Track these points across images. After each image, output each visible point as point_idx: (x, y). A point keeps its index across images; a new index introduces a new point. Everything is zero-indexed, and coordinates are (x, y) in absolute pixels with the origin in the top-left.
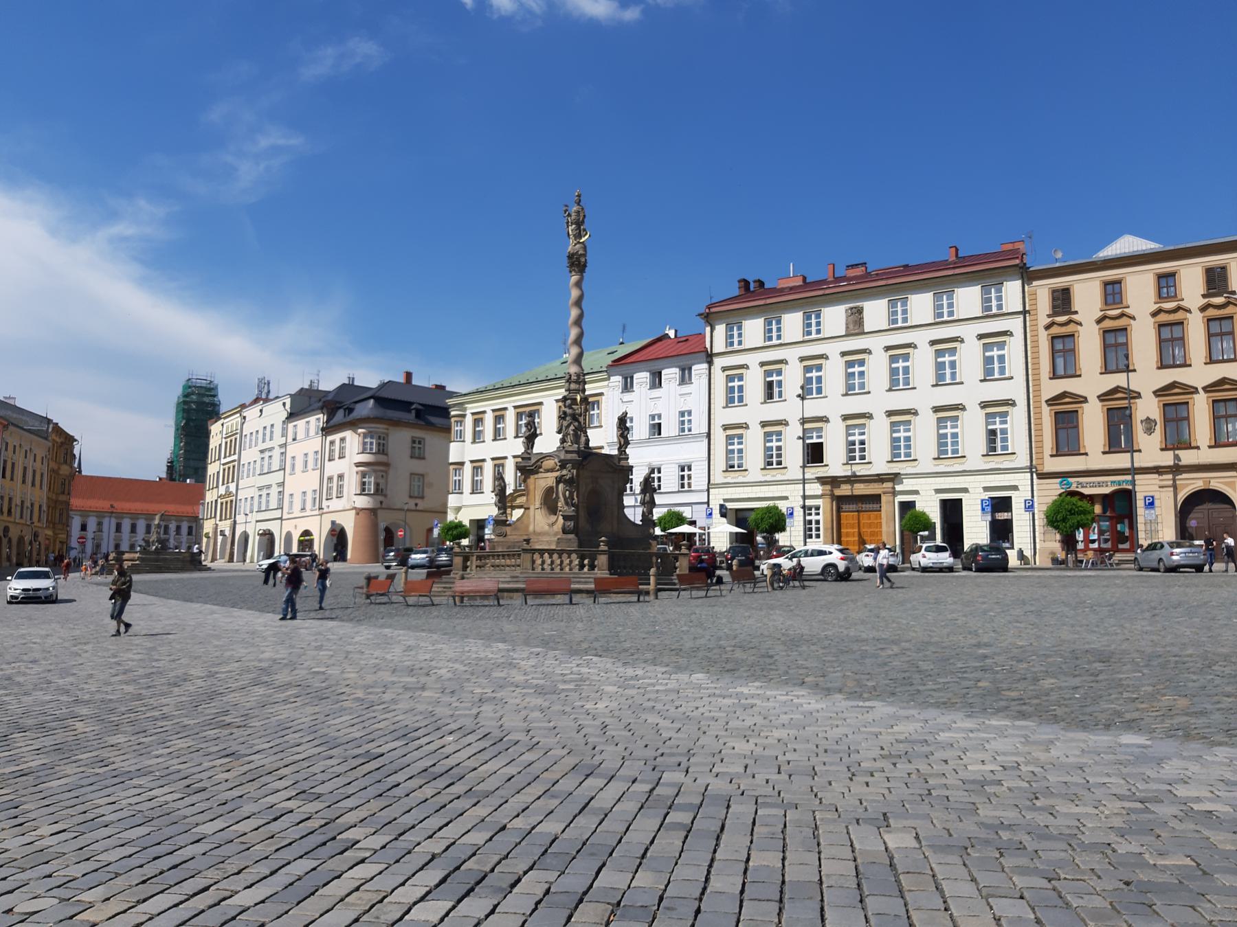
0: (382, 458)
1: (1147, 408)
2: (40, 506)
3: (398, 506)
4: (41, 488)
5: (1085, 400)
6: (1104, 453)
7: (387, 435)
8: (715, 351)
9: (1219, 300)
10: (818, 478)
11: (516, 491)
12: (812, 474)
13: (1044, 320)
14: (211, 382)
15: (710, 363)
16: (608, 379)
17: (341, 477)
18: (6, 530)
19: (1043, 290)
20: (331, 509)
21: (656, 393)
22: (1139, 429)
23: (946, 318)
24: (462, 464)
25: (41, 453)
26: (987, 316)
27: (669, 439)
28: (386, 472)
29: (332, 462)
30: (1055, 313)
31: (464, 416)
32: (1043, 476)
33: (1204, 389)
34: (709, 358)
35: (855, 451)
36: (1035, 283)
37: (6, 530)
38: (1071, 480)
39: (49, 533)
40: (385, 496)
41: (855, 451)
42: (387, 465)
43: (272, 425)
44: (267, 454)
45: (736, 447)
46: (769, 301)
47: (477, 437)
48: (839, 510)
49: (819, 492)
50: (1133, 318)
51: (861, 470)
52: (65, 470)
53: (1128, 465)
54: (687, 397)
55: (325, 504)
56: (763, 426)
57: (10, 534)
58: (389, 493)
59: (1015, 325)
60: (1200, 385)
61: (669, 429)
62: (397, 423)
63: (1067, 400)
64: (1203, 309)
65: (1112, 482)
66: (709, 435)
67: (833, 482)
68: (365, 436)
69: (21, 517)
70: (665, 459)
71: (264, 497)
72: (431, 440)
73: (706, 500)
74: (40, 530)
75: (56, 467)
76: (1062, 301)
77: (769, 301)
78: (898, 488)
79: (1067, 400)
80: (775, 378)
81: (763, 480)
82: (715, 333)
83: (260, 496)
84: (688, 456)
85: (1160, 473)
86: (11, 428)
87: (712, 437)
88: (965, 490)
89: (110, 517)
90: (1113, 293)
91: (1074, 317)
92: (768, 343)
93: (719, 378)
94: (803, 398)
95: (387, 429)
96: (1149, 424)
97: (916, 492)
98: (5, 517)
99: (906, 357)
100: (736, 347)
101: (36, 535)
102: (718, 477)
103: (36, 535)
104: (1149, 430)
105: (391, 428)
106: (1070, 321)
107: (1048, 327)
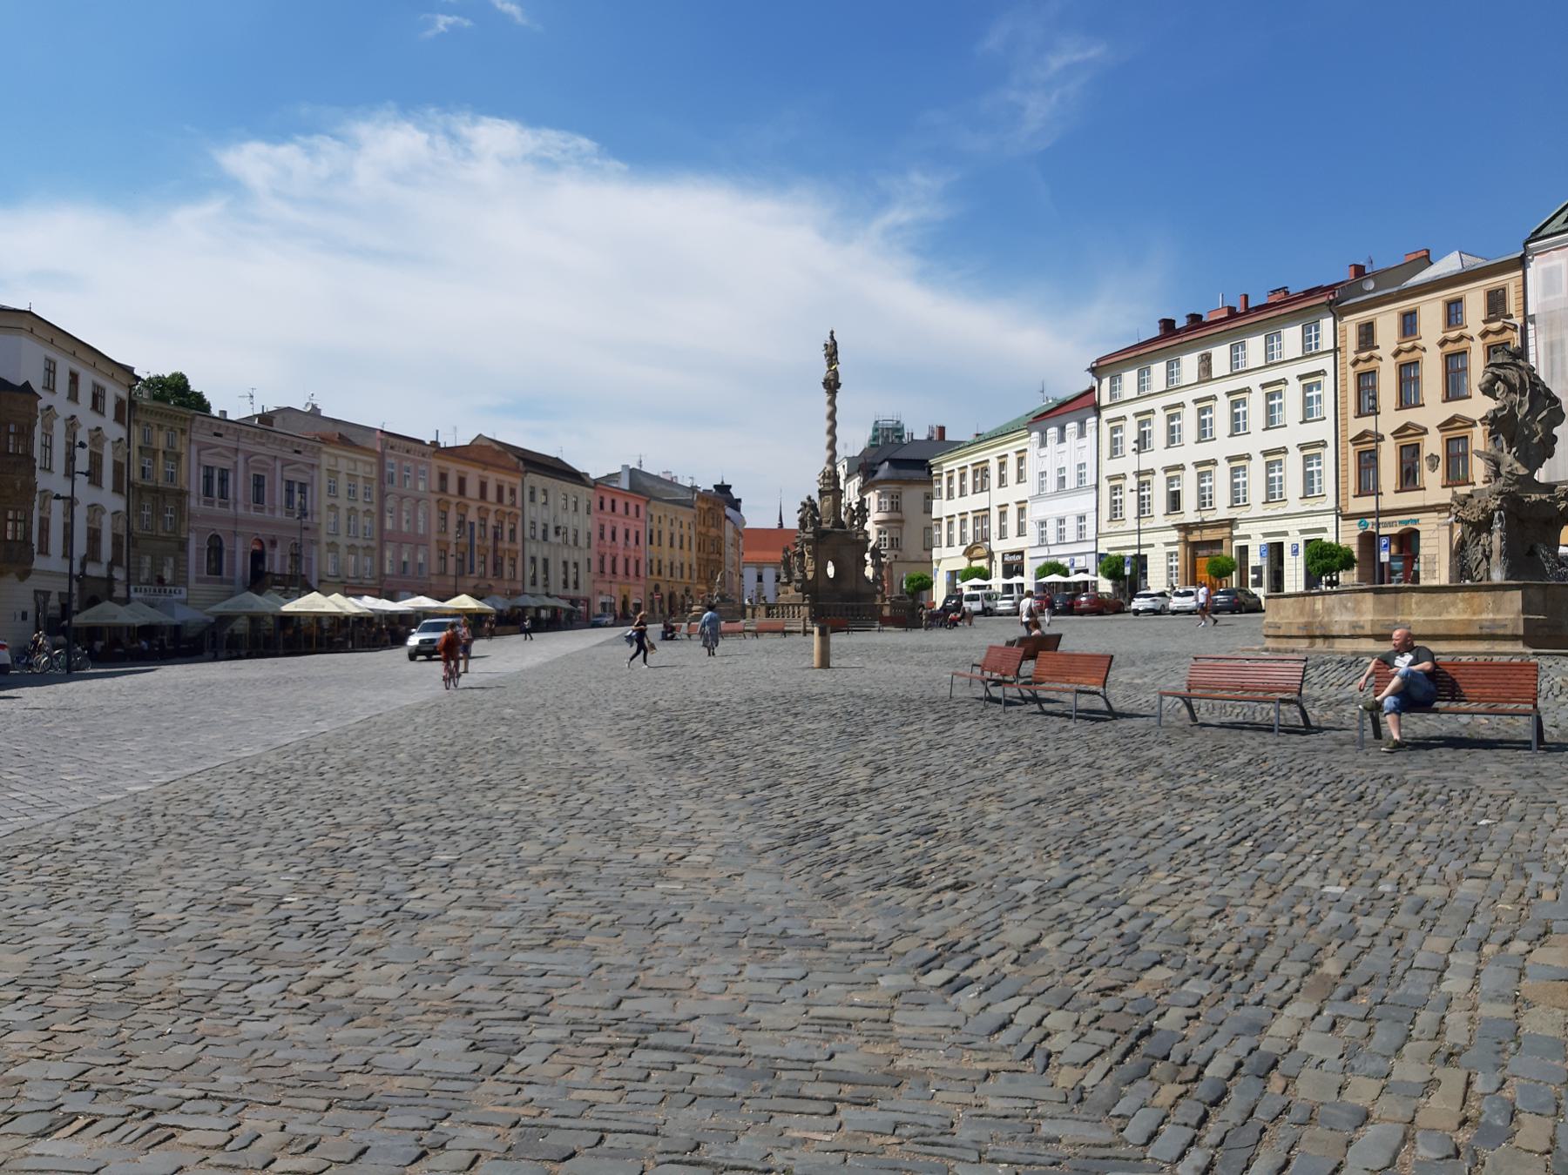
0: (896, 515)
1: (1433, 444)
2: (690, 566)
3: (913, 558)
4: (690, 549)
5: (1425, 431)
6: (1396, 492)
9: (1496, 326)
11: (974, 543)
13: (1351, 357)
14: (898, 422)
15: (1098, 415)
16: (1030, 435)
18: (657, 587)
19: (1351, 323)
22: (1424, 465)
23: (1275, 360)
24: (941, 519)
25: (686, 520)
26: (1307, 355)
27: (1071, 491)
28: (901, 529)
30: (1361, 350)
31: (941, 475)
32: (1348, 517)
33: (1481, 420)
34: (1097, 410)
35: (1204, 501)
36: (1346, 319)
37: (657, 587)
38: (1369, 520)
39: (703, 587)
40: (901, 550)
41: (1204, 501)
42: (901, 521)
45: (1277, 474)
46: (1232, 326)
47: (950, 495)
48: (1194, 556)
49: (1176, 539)
50: (1424, 350)
51: (1209, 516)
52: (713, 532)
53: (1373, 508)
56: (1302, 449)
57: (661, 591)
58: (904, 547)
59: (1326, 363)
60: (1477, 415)
61: (1071, 483)
62: (910, 482)
63: (1458, 424)
64: (1484, 335)
65: (1400, 522)
66: (1097, 487)
67: (1185, 528)
68: (880, 496)
69: (672, 575)
72: (912, 496)
74: (691, 587)
75: (703, 530)
76: (1367, 335)
77: (1232, 326)
78: (1236, 533)
79: (1458, 424)
80: (1147, 428)
82: (1102, 386)
85: (1439, 512)
86: (653, 502)
88: (1285, 534)
90: (1409, 323)
91: (1465, 331)
92: (1142, 394)
93: (1105, 429)
94: (1139, 452)
96: (1433, 459)
97: (1248, 537)
98: (655, 576)
99: (1244, 401)
101: (687, 590)
102: (1104, 528)
103: (687, 590)
104: (1433, 468)
106: (1371, 358)
107: (1355, 363)
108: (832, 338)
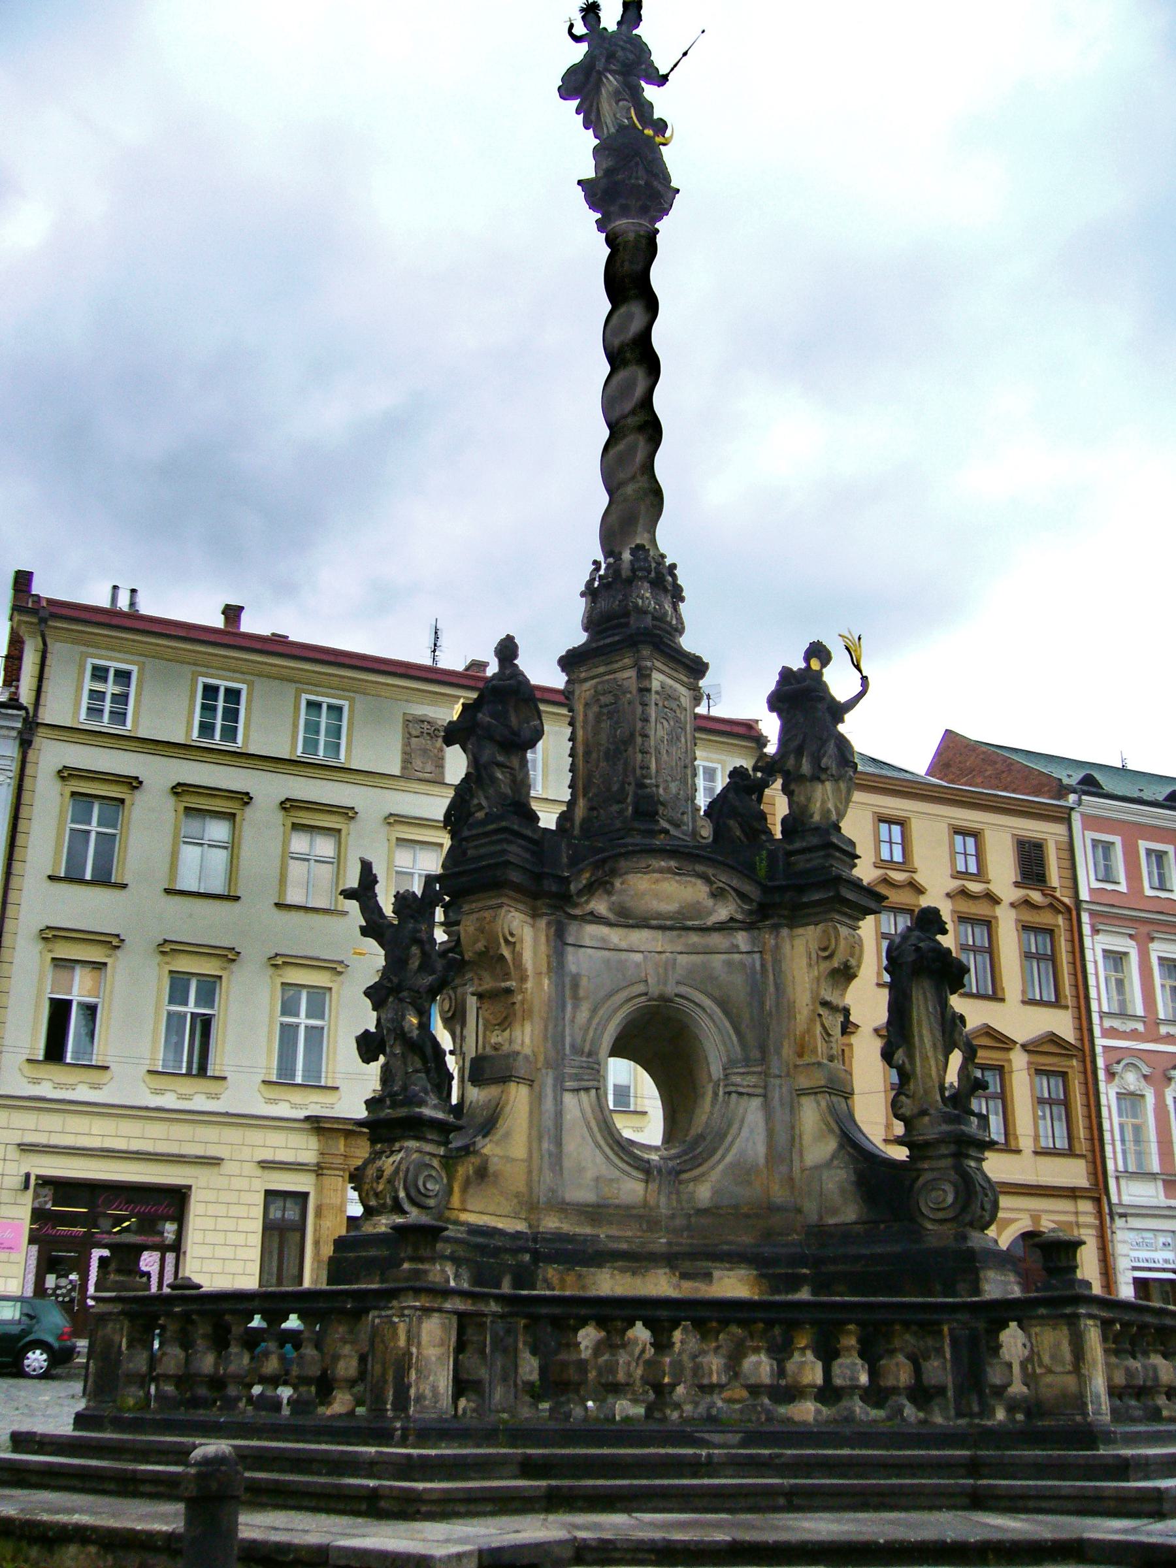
8: (48, 715)
10: (308, 1119)
12: (294, 1106)
15: (25, 745)
33: (1023, 1046)
81: (152, 1105)
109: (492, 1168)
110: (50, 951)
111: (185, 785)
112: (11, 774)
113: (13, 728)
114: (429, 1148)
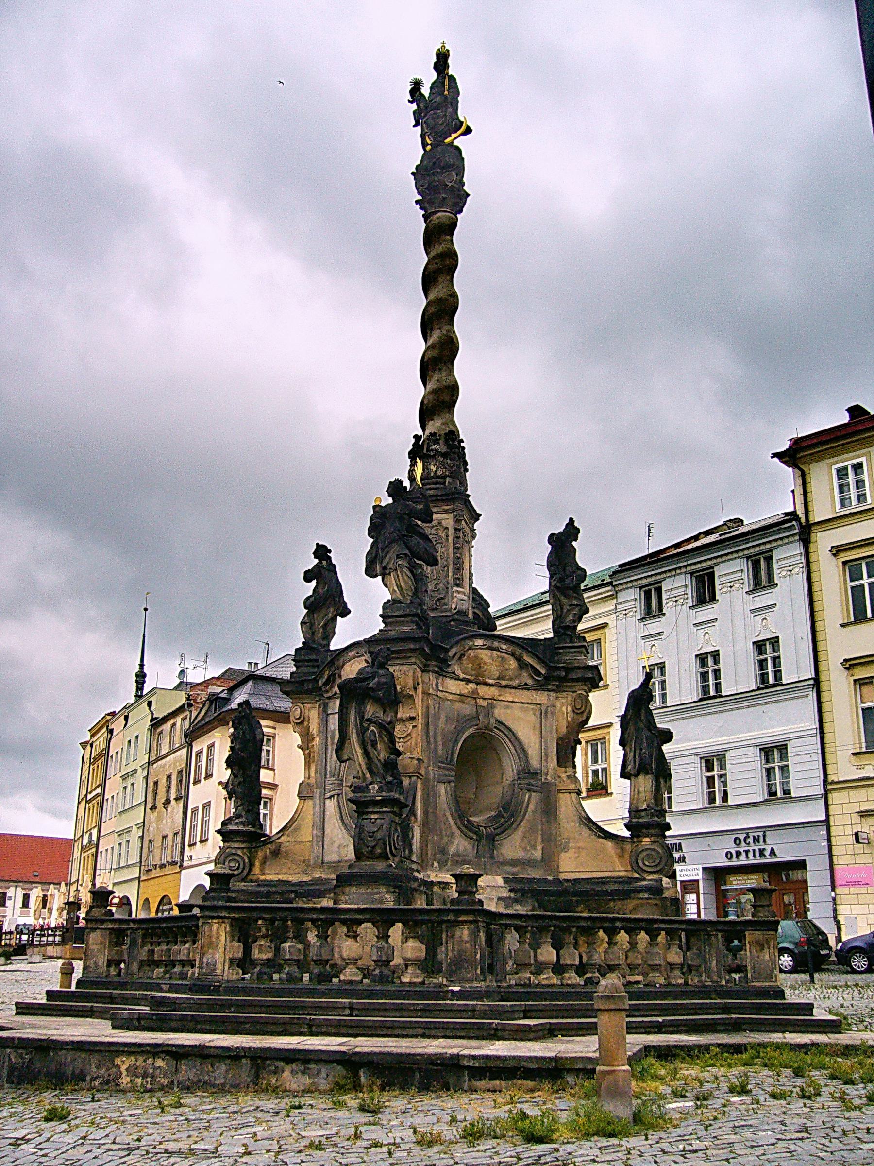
7: (274, 737)
15: (806, 542)
17: (206, 806)
20: (193, 863)
21: (706, 613)
27: (739, 698)
29: (198, 786)
43: (137, 737)
44: (130, 781)
54: (769, 616)
55: (187, 851)
66: (817, 683)
70: (732, 738)
71: (124, 845)
73: (823, 818)
83: (120, 844)
84: (778, 730)
87: (824, 687)
89: (16, 887)
95: (274, 728)
100: (854, 506)
105: (278, 725)
108: (442, 61)
109: (283, 850)
110: (852, 675)
111: (837, 547)
112: (801, 565)
113: (793, 535)
114: (236, 845)
